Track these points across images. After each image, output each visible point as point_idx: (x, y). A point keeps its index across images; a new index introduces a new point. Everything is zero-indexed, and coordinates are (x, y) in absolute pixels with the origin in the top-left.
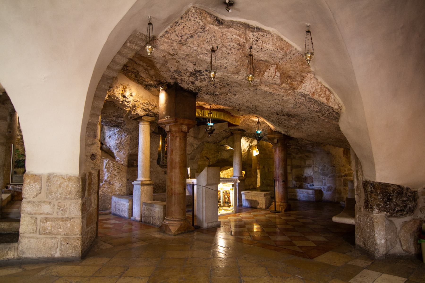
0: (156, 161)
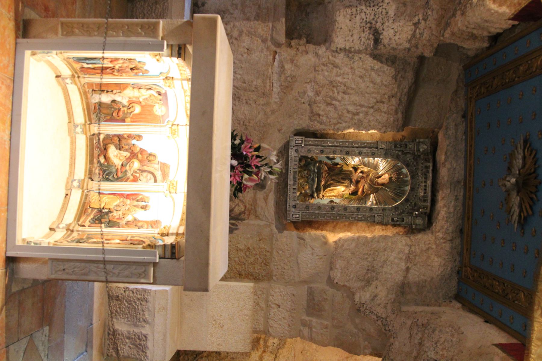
0: (304, 123)
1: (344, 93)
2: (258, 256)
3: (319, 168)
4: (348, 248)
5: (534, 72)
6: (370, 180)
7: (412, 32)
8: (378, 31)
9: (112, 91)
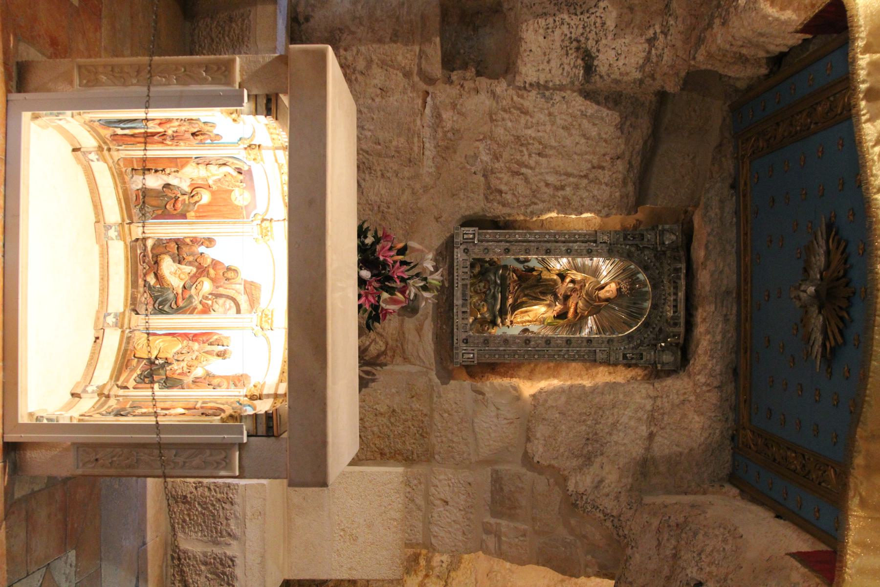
0: (476, 205)
1: (539, 154)
2: (409, 423)
3: (503, 278)
4: (554, 405)
5: (840, 115)
6: (587, 294)
7: (646, 54)
8: (590, 53)
9: (163, 170)
